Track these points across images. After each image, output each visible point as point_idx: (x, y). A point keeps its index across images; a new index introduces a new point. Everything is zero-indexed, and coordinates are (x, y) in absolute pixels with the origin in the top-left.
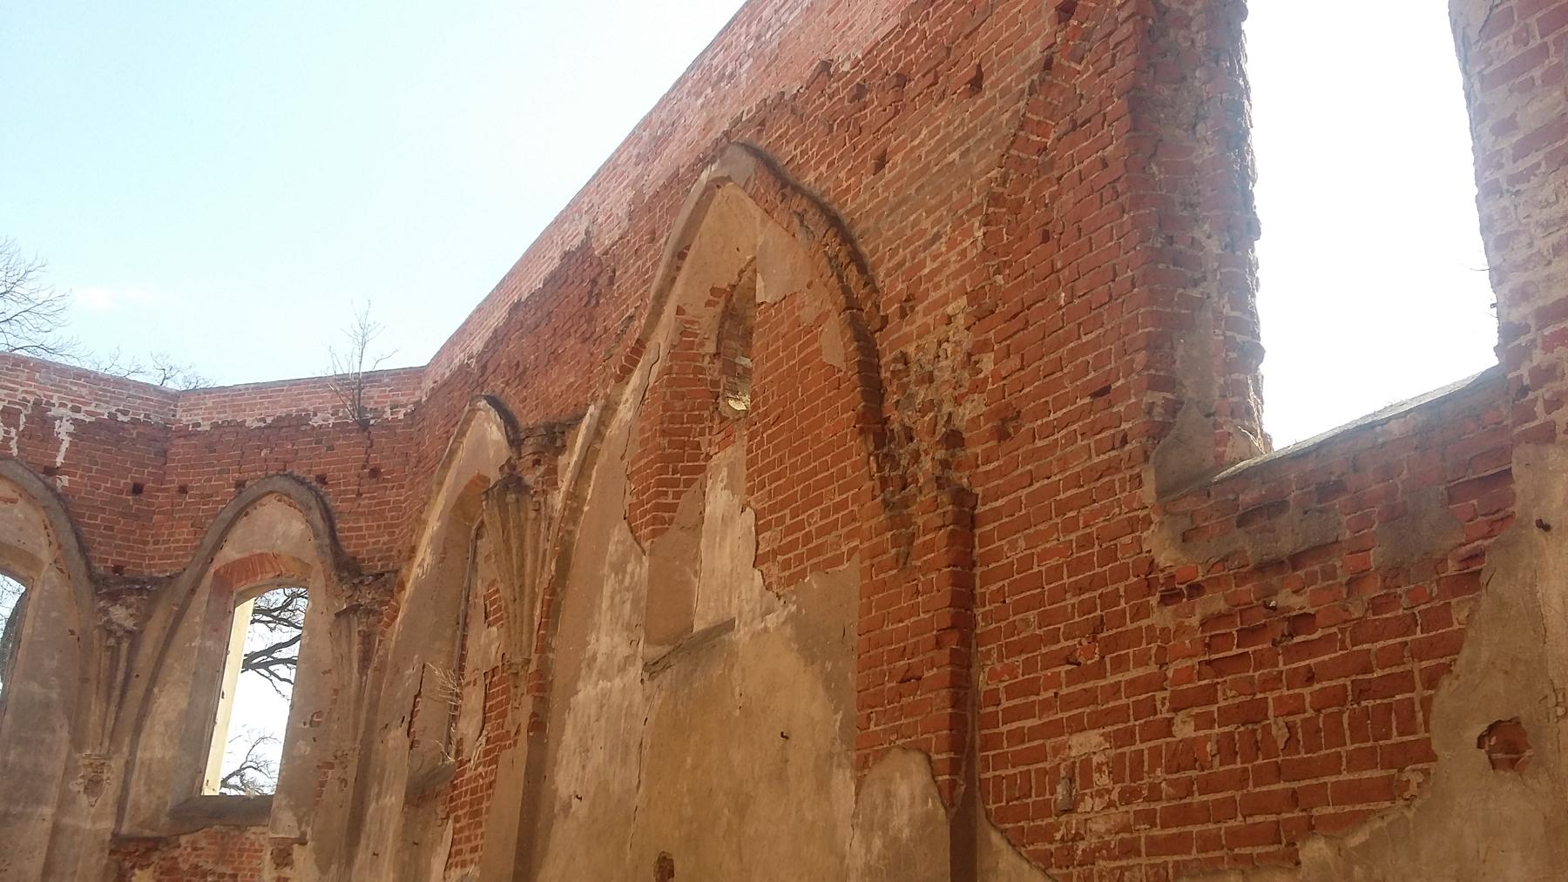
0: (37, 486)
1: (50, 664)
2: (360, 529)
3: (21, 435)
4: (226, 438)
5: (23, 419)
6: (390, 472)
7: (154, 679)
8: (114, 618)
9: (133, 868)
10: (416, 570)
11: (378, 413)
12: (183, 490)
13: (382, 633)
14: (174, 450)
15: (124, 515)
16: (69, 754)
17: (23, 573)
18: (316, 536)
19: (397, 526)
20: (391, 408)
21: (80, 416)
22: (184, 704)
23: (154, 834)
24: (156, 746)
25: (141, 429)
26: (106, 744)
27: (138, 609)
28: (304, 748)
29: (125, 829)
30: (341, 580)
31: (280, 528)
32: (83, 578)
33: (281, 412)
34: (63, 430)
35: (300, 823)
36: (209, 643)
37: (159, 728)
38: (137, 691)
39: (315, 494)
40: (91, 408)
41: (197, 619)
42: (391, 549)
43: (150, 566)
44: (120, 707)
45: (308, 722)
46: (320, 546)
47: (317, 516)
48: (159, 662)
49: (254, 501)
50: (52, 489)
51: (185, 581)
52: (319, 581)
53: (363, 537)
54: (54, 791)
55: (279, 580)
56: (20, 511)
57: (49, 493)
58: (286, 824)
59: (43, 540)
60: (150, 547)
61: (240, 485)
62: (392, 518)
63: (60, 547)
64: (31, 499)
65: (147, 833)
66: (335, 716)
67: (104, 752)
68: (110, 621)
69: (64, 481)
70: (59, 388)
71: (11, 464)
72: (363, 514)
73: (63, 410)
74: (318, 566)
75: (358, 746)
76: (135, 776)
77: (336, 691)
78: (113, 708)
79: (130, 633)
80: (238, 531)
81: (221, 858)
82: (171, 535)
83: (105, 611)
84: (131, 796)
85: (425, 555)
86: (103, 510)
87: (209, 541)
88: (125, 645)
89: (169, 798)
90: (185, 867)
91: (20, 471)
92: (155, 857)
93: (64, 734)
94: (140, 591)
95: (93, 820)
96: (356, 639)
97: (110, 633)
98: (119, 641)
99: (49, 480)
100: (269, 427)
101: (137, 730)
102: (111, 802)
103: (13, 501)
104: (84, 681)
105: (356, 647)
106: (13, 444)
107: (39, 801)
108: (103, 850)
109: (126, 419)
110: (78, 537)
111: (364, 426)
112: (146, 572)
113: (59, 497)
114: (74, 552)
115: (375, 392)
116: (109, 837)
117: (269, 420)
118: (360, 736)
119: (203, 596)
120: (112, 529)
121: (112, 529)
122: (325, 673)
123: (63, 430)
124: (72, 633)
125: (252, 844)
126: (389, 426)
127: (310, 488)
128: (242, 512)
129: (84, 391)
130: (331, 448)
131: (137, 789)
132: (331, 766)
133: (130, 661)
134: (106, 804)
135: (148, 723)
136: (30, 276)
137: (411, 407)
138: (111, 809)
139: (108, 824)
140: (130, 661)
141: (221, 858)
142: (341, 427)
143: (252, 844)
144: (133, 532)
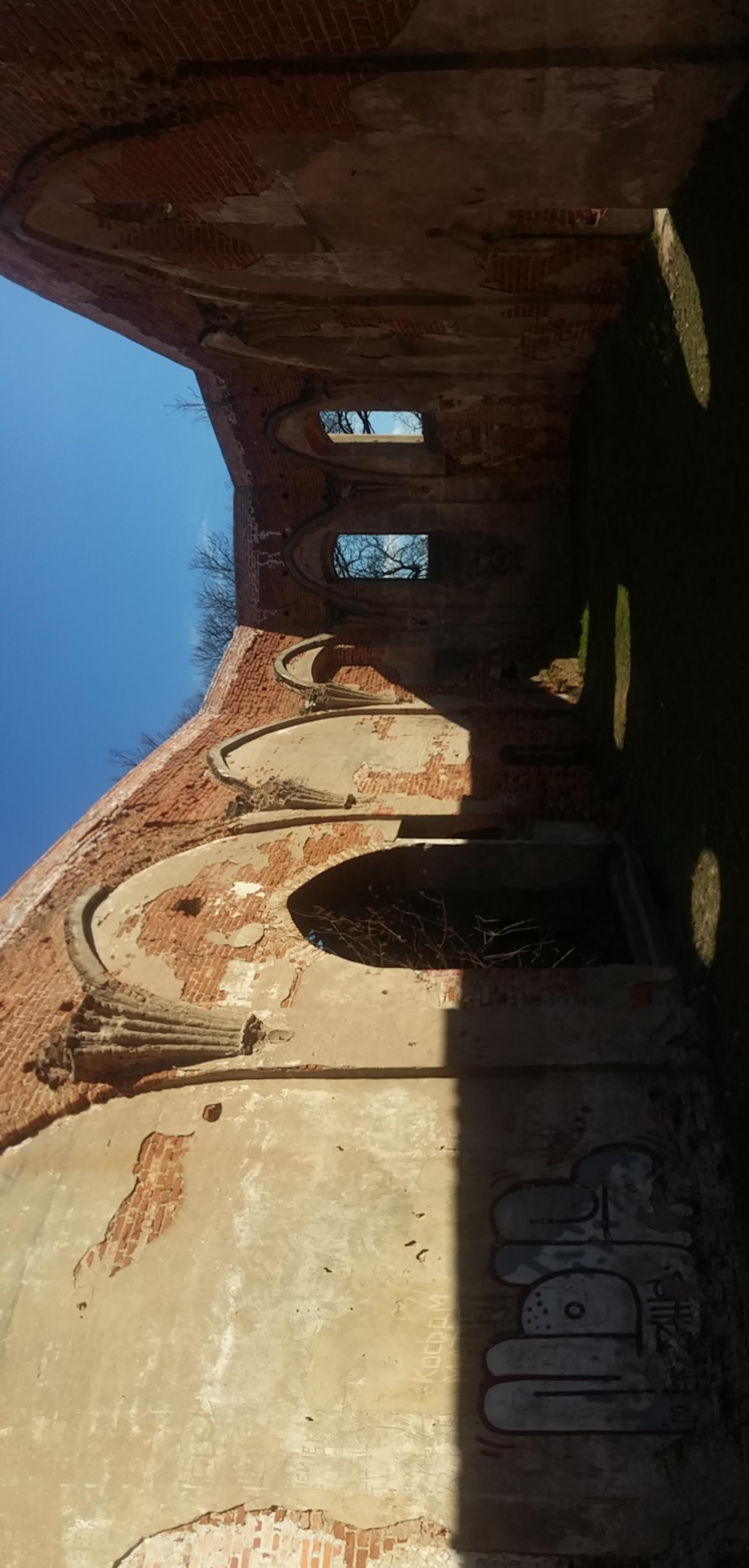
10: (301, 364)
24: (405, 466)
34: (264, 535)
50: (293, 534)
73: (256, 537)
83: (344, 500)
85: (291, 361)
88: (359, 488)
123: (264, 535)
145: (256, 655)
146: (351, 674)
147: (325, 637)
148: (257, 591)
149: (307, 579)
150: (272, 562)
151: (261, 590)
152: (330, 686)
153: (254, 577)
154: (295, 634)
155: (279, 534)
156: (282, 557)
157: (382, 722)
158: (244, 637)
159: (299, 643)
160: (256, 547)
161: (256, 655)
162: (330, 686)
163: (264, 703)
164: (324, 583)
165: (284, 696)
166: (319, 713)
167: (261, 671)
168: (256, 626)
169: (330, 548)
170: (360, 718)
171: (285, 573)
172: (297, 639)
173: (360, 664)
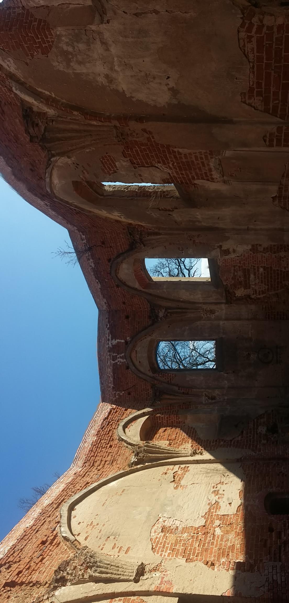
7: (179, 301)
9: (235, 297)
16: (204, 320)
22: (184, 291)
23: (224, 292)
24: (198, 297)
26: (199, 310)
29: (224, 301)
37: (192, 297)
48: (173, 300)
50: (131, 341)
56: (138, 349)
61: (118, 286)
65: (224, 294)
68: (163, 317)
78: (188, 311)
79: (166, 310)
83: (161, 319)
84: (214, 301)
88: (169, 311)
90: (233, 282)
93: (198, 323)
95: (223, 310)
97: (167, 315)
98: (168, 313)
116: (227, 305)
124: (169, 327)
139: (223, 306)
145: (109, 422)
154: (133, 408)
155: (123, 341)
161: (109, 422)
167: (110, 434)
168: (112, 403)
169: (153, 350)
172: (134, 411)
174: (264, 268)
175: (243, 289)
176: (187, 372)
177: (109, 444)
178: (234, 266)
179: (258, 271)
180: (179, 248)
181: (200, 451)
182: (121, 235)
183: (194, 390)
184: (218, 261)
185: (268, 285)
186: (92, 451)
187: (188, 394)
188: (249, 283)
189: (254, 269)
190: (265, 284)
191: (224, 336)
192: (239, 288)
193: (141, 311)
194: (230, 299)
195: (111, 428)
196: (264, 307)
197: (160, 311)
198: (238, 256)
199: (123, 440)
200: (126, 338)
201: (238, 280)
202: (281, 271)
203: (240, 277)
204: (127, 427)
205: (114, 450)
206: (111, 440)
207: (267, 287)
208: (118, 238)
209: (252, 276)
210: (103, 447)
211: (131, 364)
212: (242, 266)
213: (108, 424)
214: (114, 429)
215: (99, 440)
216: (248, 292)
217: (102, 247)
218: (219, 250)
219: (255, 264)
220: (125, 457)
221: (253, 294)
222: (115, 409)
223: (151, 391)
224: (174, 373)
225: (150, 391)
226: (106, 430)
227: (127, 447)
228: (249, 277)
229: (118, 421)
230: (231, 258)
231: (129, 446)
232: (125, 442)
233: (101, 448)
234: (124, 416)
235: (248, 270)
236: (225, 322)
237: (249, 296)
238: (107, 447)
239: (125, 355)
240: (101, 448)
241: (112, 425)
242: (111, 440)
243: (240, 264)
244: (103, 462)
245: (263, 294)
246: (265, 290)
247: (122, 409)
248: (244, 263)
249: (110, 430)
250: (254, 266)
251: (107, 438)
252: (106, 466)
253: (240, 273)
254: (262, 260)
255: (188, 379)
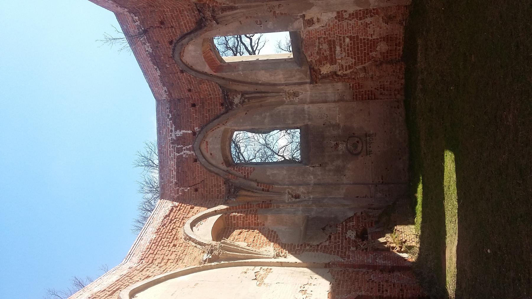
0: (200, 136)
1: (258, 118)
2: (185, 23)
3: (184, 145)
4: (167, 80)
5: (179, 146)
6: (160, 17)
7: (257, 84)
8: (238, 102)
9: (321, 74)
11: (139, 27)
12: (190, 90)
13: (220, 4)
14: (177, 97)
15: (203, 108)
16: (287, 105)
17: (230, 133)
18: (192, 39)
19: (179, 9)
20: (135, 22)
21: (173, 129)
22: (263, 72)
24: (279, 77)
25: (172, 109)
26: (281, 94)
27: (234, 95)
28: (270, 25)
29: (308, 80)
30: (205, 26)
31: (193, 53)
32: (227, 114)
33: (151, 64)
34: (179, 133)
35: (297, 19)
36: (240, 68)
37: (273, 78)
38: (262, 88)
39: (177, 44)
40: (170, 126)
41: (233, 74)
42: (189, 9)
43: (219, 94)
44: (268, 93)
45: (264, 26)
46: (195, 37)
47: (184, 41)
48: (251, 83)
49: (186, 65)
50: (200, 132)
51: (222, 82)
52: (208, 34)
53: (187, 21)
54: (299, 107)
55: (212, 49)
56: (209, 139)
57: (202, 132)
58: (298, 24)
59: (217, 130)
60: (212, 96)
61: (182, 72)
62: (177, 12)
63: (218, 125)
64: (205, 137)
65: (308, 73)
66: (256, 15)
67: (284, 94)
68: (240, 103)
69: (197, 129)
70: (165, 138)
71: (195, 146)
72: (179, 24)
73: (173, 135)
74: (203, 36)
75: (265, 3)
76: (291, 82)
77: (247, 17)
78: (269, 95)
79: (242, 95)
80: (198, 68)
81: (313, 45)
82: (206, 90)
83: (237, 105)
86: (203, 114)
87: (204, 77)
88: (247, 96)
89: (296, 69)
90: (318, 57)
91: (196, 143)
92: (316, 68)
93: (280, 108)
94: (228, 96)
95: (307, 91)
96: (225, 13)
99: (197, 133)
100: (158, 67)
101: (275, 85)
102: (300, 87)
103: (207, 142)
104: (261, 106)
105: (228, 13)
106: (188, 147)
107: (303, 110)
108: (316, 86)
109: (170, 115)
110: (214, 120)
111: (145, 32)
112: (221, 95)
113: (202, 129)
114: (219, 119)
115: (131, 30)
116: (312, 85)
117: (156, 67)
118: (260, 3)
119: (224, 75)
120: (209, 110)
121: (209, 110)
122: (241, 24)
123: (179, 133)
124: (246, 114)
125: (307, 35)
126: (142, 22)
127: (175, 46)
128: (191, 68)
129: (164, 130)
130: (158, 42)
131: (295, 80)
132: (274, 12)
133: (252, 93)
134: (301, 89)
135: (273, 82)
136: (143, 155)
137: (132, 15)
138: (302, 87)
139: (308, 87)
140: (252, 93)
141: (313, 45)
142: (149, 40)
143: (307, 35)
144: (209, 103)
145: (172, 220)
146: (242, 235)
147: (223, 207)
148: (175, 173)
149: (210, 163)
150: (186, 152)
151: (178, 172)
152: (223, 243)
153: (172, 163)
154: (201, 205)
155: (190, 132)
156: (193, 149)
157: (262, 272)
158: (165, 206)
159: (205, 211)
160: (174, 142)
161: (172, 220)
162: (223, 243)
163: (173, 256)
164: (224, 167)
165: (190, 250)
166: (213, 264)
167: (174, 233)
168: (174, 200)
169: (227, 140)
170: (245, 268)
171: (196, 160)
172: (203, 208)
173: (249, 227)
174: (351, 38)
175: (328, 65)
176: (267, 166)
177: (173, 244)
178: (319, 38)
179: (344, 41)
180: (257, 22)
181: (284, 254)
182: (185, 12)
183: (276, 186)
184: (302, 34)
185: (355, 58)
186: (150, 248)
187: (268, 191)
188: (335, 57)
189: (340, 40)
190: (352, 58)
191: (309, 123)
192: (324, 65)
193: (211, 98)
194: (315, 77)
195: (175, 227)
196: (351, 85)
197: (235, 97)
198: (322, 27)
199: (190, 239)
200: (194, 128)
201: (323, 54)
202: (368, 40)
203: (325, 51)
204: (195, 226)
205: (179, 249)
206: (175, 238)
207: (354, 60)
208: (182, 16)
209: (338, 48)
210: (165, 245)
211: (200, 156)
212: (327, 38)
213: (170, 222)
214: (179, 227)
215: (160, 238)
216: (335, 68)
217: (161, 28)
218: (301, 20)
219: (341, 34)
220: (193, 257)
221: (340, 70)
222: (177, 207)
223: (223, 188)
224: (252, 166)
225: (223, 188)
226: (168, 228)
227: (196, 247)
228: (335, 51)
229: (183, 219)
230: (316, 30)
231: (199, 246)
232: (193, 241)
233: (162, 246)
234: (190, 214)
235: (334, 41)
236: (311, 105)
237: (335, 73)
238: (169, 246)
239: (193, 147)
240: (162, 246)
241: (175, 223)
242: (175, 238)
243: (325, 35)
244: (165, 261)
245: (349, 69)
246: (352, 64)
247: (187, 207)
248: (329, 33)
249: (173, 228)
250: (340, 37)
251: (169, 237)
252: (169, 264)
253: (325, 46)
254: (348, 29)
255: (268, 173)
